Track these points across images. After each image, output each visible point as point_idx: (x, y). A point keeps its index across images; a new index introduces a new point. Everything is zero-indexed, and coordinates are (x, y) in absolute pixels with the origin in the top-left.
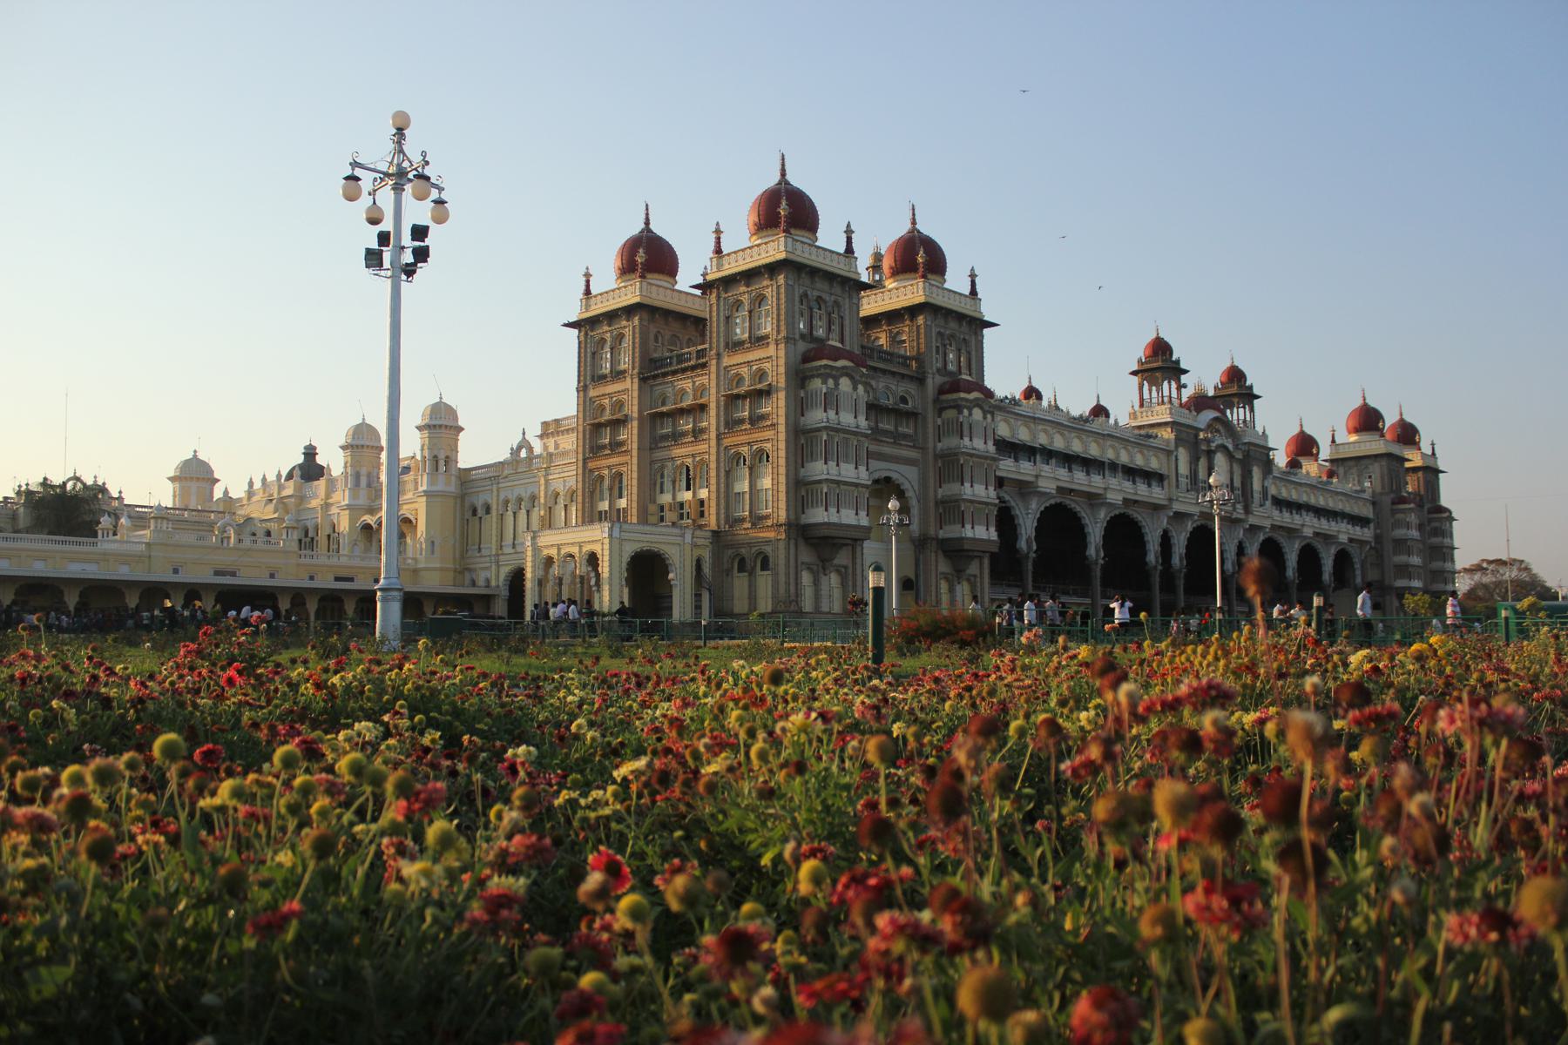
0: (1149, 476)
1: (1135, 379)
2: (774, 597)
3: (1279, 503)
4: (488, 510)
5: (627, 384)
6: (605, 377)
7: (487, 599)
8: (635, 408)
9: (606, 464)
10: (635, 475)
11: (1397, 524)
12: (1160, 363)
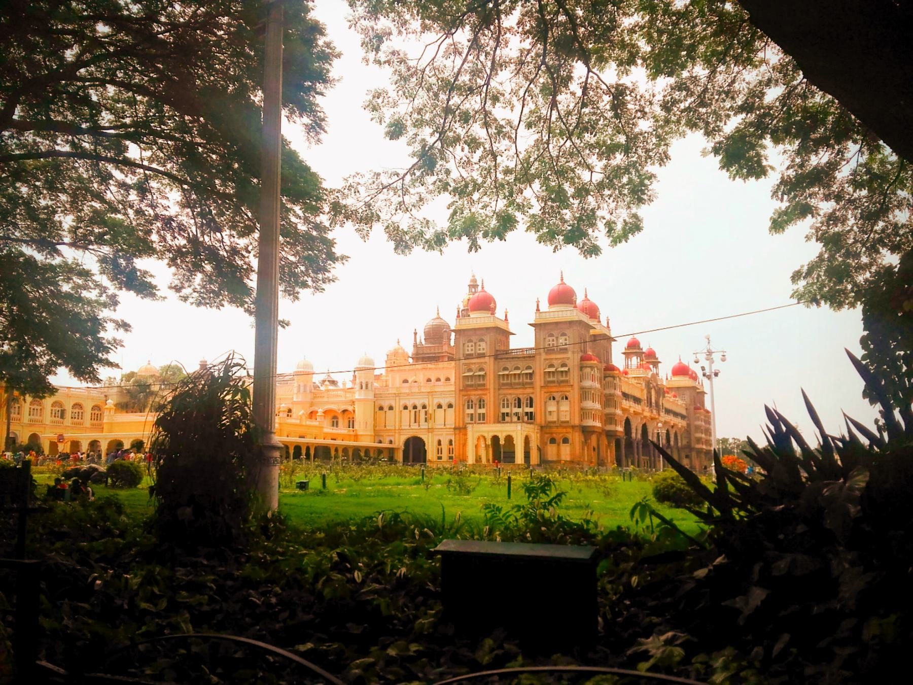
0: (637, 400)
1: (624, 356)
2: (572, 454)
3: (668, 411)
4: (391, 408)
5: (487, 359)
6: (471, 355)
7: (391, 451)
8: (492, 371)
9: (474, 396)
10: (492, 399)
11: (698, 419)
12: (633, 348)
